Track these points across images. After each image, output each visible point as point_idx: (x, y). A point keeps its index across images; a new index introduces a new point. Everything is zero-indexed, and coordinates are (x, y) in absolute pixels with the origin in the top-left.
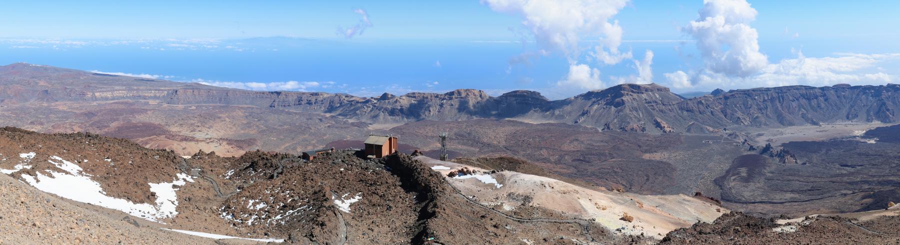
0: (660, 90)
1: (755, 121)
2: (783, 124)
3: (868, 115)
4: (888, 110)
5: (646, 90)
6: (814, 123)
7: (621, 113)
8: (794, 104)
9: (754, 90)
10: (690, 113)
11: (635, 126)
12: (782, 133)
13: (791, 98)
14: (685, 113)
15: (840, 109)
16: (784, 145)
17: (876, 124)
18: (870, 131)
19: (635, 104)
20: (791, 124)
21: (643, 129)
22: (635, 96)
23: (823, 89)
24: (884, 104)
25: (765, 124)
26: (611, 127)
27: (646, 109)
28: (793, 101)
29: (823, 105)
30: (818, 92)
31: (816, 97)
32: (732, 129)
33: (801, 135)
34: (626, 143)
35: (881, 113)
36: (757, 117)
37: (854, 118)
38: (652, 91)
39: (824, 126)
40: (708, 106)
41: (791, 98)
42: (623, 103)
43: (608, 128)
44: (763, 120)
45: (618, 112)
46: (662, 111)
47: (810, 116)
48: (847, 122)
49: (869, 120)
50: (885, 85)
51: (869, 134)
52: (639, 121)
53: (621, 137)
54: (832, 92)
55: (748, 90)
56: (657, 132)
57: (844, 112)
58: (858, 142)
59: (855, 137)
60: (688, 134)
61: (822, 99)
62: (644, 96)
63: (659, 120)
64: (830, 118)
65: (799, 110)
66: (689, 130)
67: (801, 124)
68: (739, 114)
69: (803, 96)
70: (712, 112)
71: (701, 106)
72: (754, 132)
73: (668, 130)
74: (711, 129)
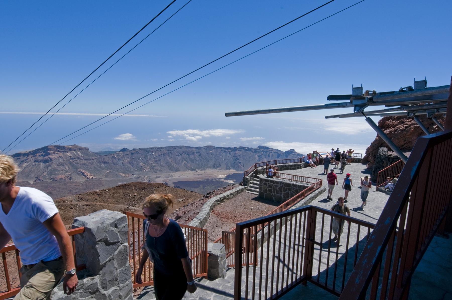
0: (81, 149)
1: (153, 169)
2: (172, 170)
3: (227, 164)
4: (240, 163)
5: (70, 149)
6: (193, 170)
7: (50, 168)
8: (179, 158)
9: (151, 148)
10: (106, 165)
11: (63, 176)
12: (172, 176)
13: (177, 154)
14: (102, 165)
15: (209, 161)
16: (174, 183)
17: (232, 171)
18: (229, 175)
19: (61, 161)
20: (177, 170)
21: (71, 178)
22: (61, 154)
23: (197, 148)
24: (237, 159)
25: (160, 171)
26: (41, 178)
27: (71, 163)
28: (178, 156)
29: (197, 159)
30: (195, 151)
31: (193, 154)
32: (138, 175)
33: (185, 177)
34: (58, 190)
35: (235, 164)
36: (154, 166)
37: (218, 167)
38: (75, 150)
39: (199, 171)
40: (119, 160)
41: (177, 154)
42: (51, 160)
43: (39, 180)
44: (159, 168)
46: (84, 164)
47: (189, 165)
48: (214, 170)
49: (228, 168)
50: (238, 147)
51: (229, 177)
52: (66, 172)
53: (52, 185)
54: (204, 150)
55: (148, 149)
56: (82, 180)
57: (211, 163)
58: (222, 182)
59: (220, 179)
60: (107, 179)
61: (197, 155)
62: (69, 154)
63: (83, 171)
64: (203, 167)
65: (182, 161)
66: (107, 176)
67: (184, 171)
68: (142, 164)
69: (185, 153)
70: (123, 164)
71: (114, 160)
72: (153, 176)
73: (91, 177)
74: (123, 175)
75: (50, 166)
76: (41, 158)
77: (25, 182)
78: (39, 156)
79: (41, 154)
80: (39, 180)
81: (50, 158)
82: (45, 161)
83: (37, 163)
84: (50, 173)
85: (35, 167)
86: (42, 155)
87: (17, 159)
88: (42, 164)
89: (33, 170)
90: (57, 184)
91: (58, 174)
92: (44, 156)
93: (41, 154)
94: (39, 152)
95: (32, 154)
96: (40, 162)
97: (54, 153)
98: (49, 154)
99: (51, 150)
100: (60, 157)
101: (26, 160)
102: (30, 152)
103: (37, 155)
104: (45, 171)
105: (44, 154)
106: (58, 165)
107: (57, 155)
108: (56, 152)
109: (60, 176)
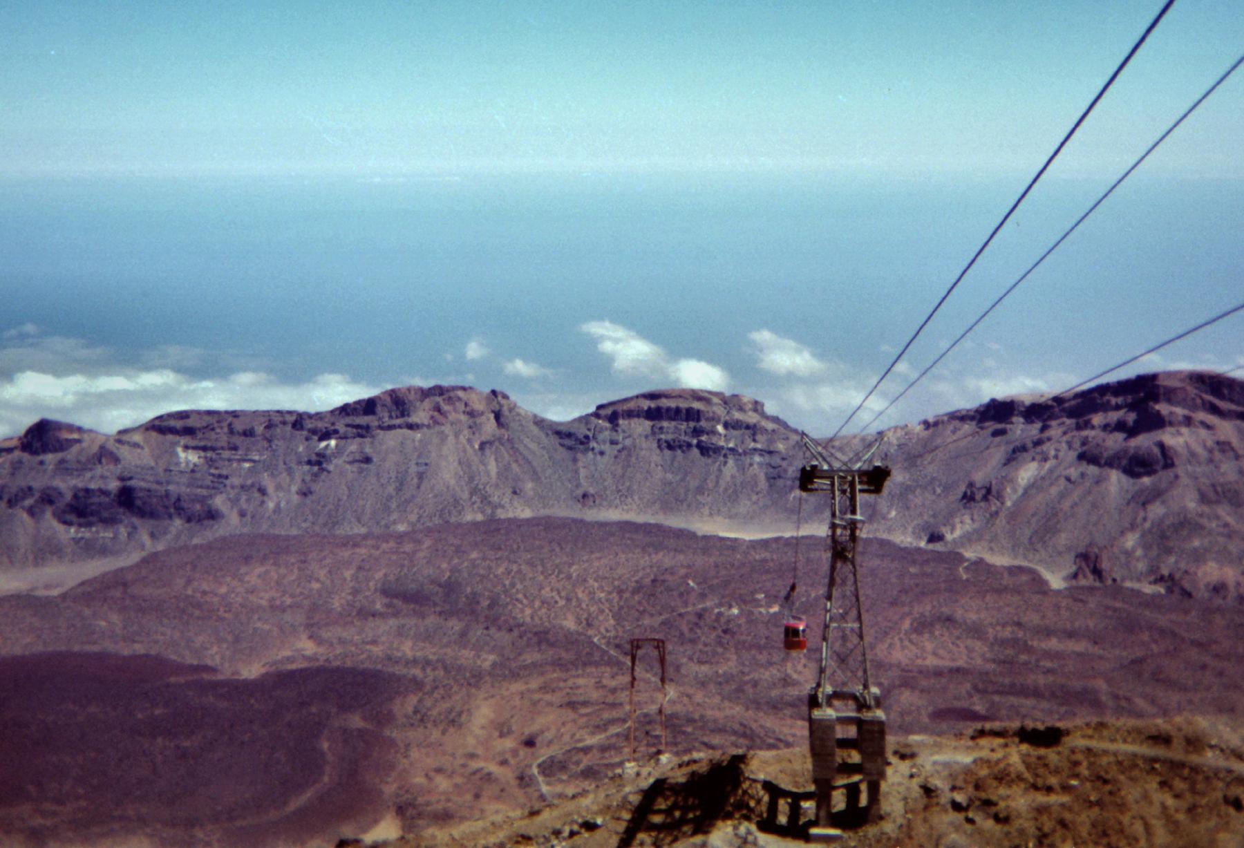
26: (1105, 565)
34: (1194, 654)
42: (1167, 458)
43: (1097, 573)
45: (1144, 500)
75: (1156, 494)
76: (1115, 441)
77: (1021, 569)
78: (1105, 427)
79: (1114, 416)
80: (1097, 573)
81: (1161, 446)
82: (1137, 466)
83: (1092, 470)
84: (1163, 538)
85: (1076, 495)
86: (1120, 426)
87: (996, 433)
88: (1116, 480)
89: (1066, 505)
90: (1193, 617)
91: (1198, 557)
92: (1132, 432)
93: (1114, 416)
94: (1106, 408)
95: (1072, 413)
96: (1110, 463)
97: (1188, 421)
98: (1159, 422)
99: (1169, 401)
100: (1224, 446)
101: (1038, 443)
102: (1058, 400)
103: (1097, 419)
104: (1133, 527)
105: (1131, 418)
106: (1203, 499)
107: (1203, 432)
108: (1201, 416)
109: (1211, 571)
